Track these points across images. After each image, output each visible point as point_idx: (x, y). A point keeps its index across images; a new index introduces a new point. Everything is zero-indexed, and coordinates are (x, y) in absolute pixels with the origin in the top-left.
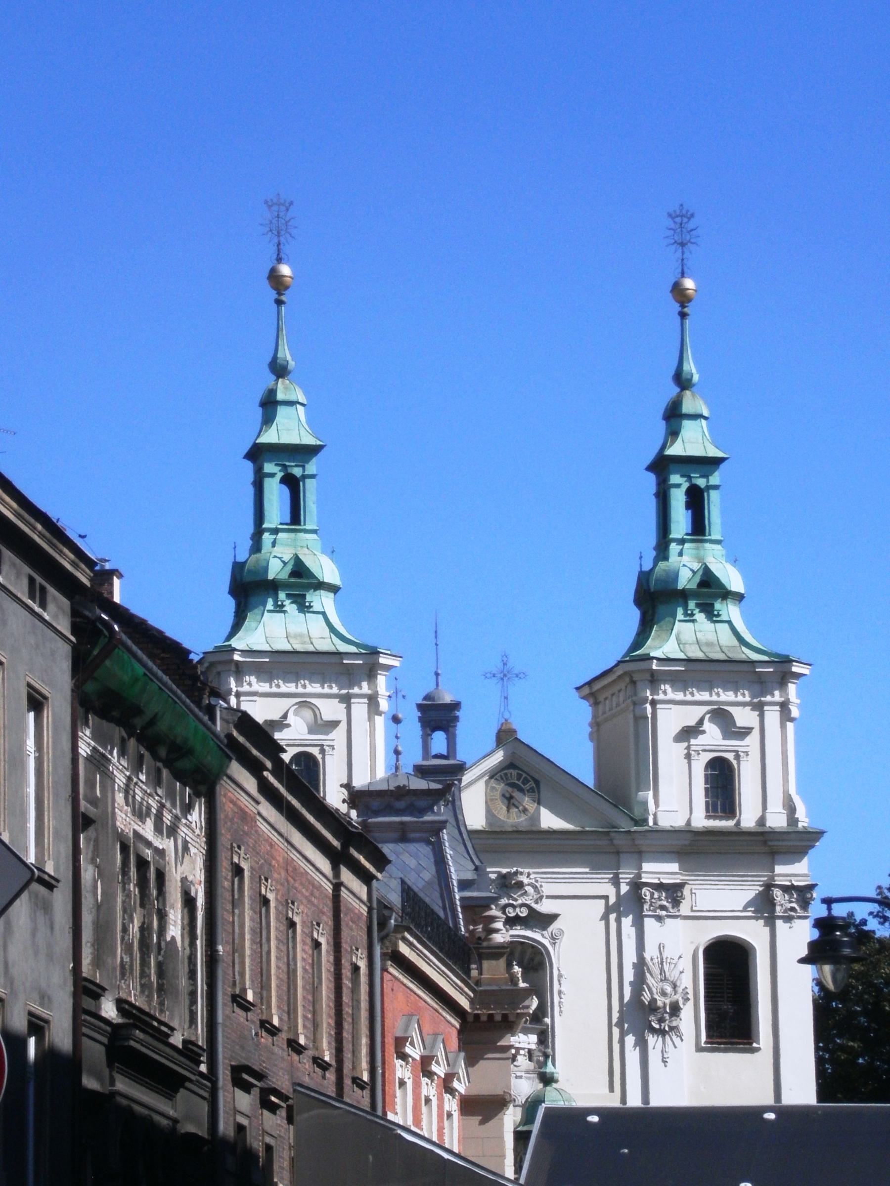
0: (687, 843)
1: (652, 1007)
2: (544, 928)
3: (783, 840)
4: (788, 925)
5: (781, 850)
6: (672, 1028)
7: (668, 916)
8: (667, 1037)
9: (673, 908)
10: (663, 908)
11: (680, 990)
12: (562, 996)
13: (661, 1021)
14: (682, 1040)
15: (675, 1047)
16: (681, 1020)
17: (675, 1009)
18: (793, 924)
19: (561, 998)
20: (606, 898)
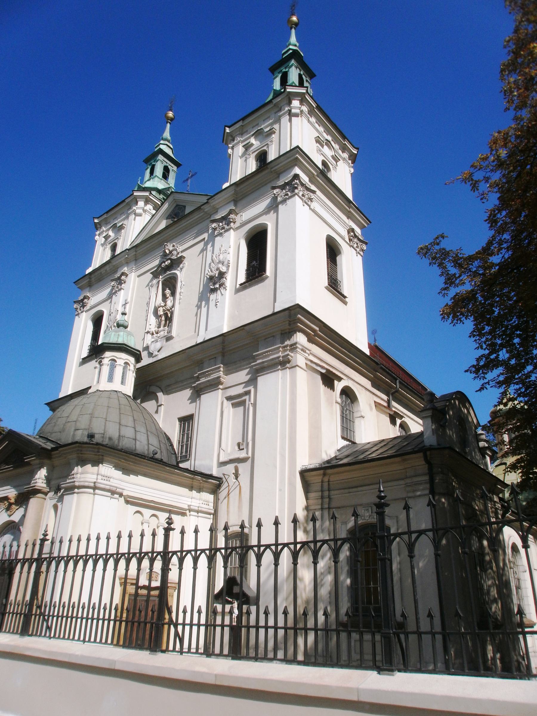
0: (233, 192)
1: (211, 278)
2: (179, 266)
3: (278, 164)
4: (286, 203)
5: (282, 171)
6: (220, 286)
7: (226, 231)
8: (219, 291)
9: (228, 226)
10: (223, 228)
11: (226, 263)
12: (181, 294)
13: (214, 284)
14: (226, 290)
15: (222, 295)
16: (226, 279)
17: (222, 275)
18: (288, 202)
19: (180, 295)
20: (204, 239)
